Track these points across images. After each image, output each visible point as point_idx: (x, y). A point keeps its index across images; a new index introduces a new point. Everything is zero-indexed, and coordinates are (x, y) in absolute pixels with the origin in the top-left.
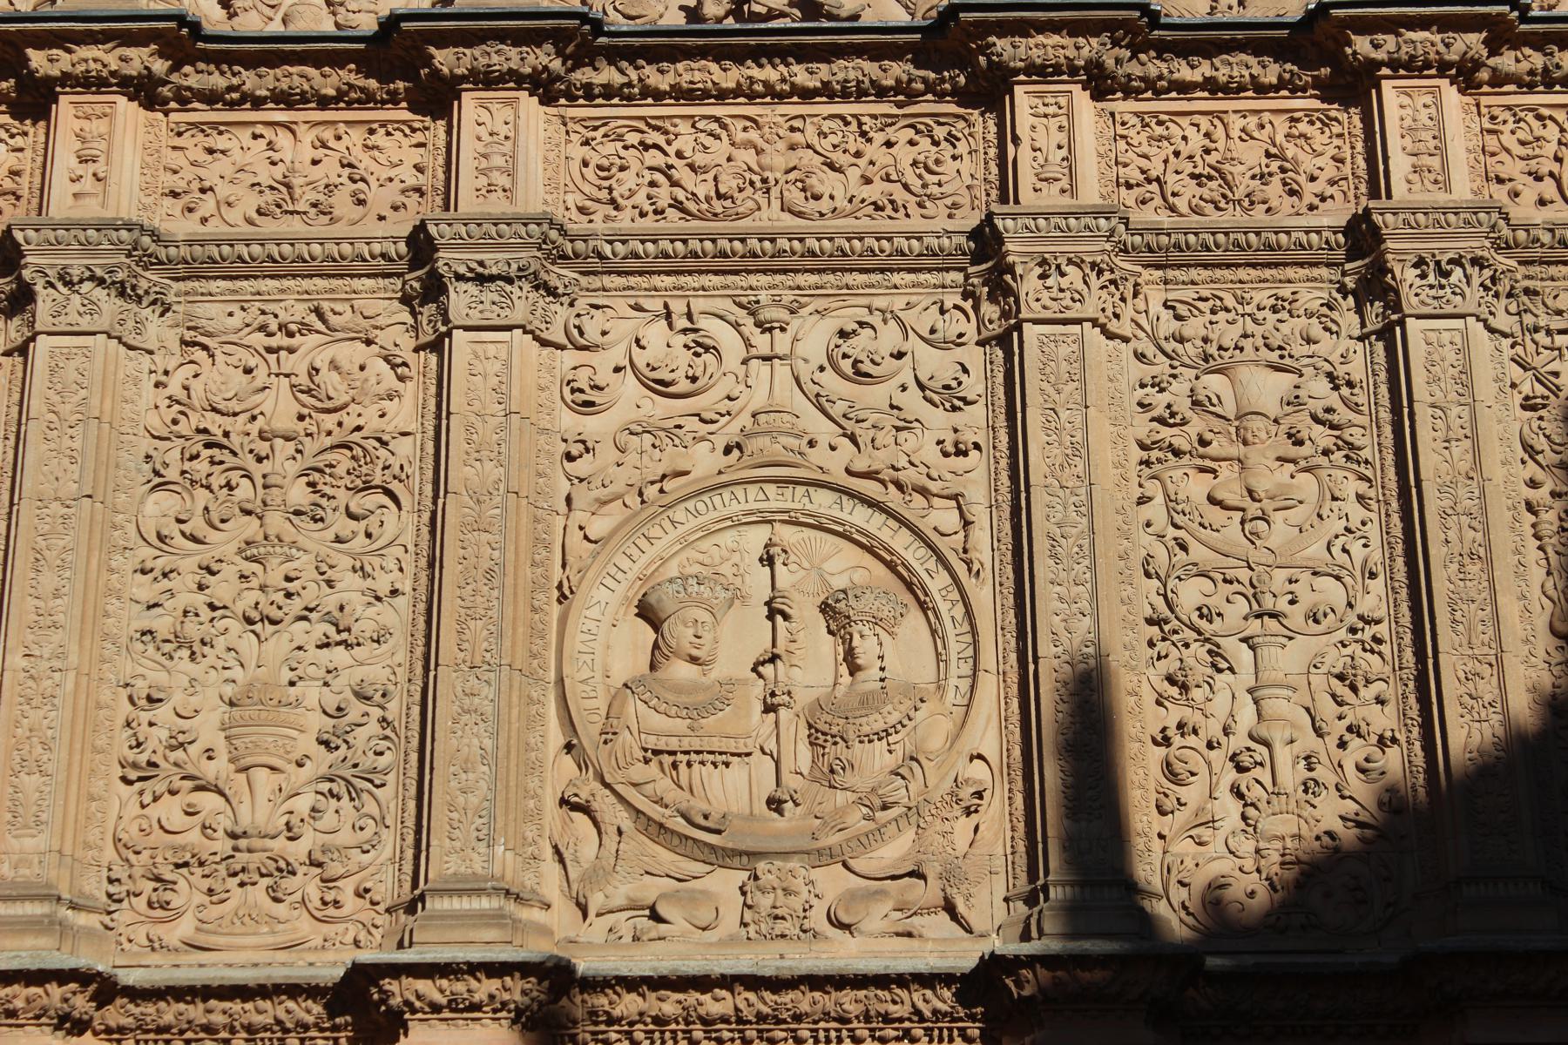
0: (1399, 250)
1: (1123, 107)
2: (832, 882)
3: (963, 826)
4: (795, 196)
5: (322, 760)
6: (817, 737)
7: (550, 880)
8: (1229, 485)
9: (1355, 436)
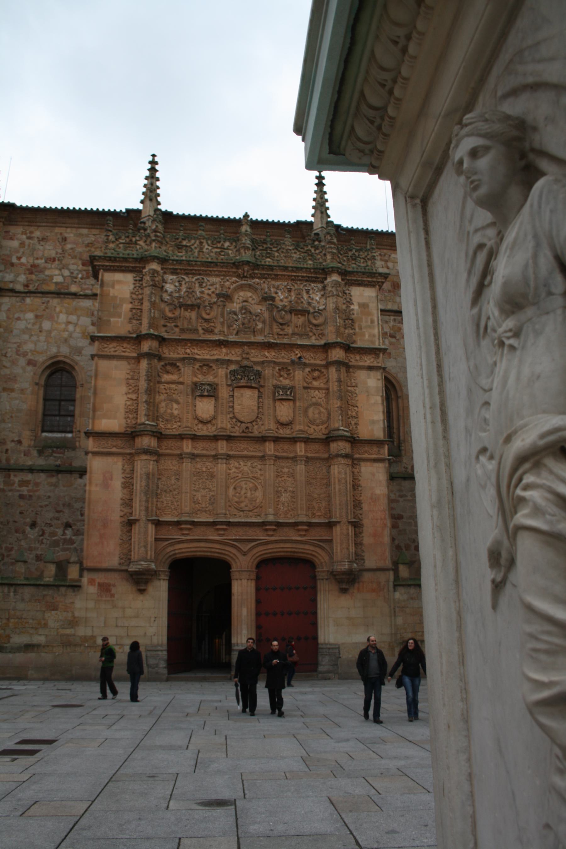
2: (251, 513)
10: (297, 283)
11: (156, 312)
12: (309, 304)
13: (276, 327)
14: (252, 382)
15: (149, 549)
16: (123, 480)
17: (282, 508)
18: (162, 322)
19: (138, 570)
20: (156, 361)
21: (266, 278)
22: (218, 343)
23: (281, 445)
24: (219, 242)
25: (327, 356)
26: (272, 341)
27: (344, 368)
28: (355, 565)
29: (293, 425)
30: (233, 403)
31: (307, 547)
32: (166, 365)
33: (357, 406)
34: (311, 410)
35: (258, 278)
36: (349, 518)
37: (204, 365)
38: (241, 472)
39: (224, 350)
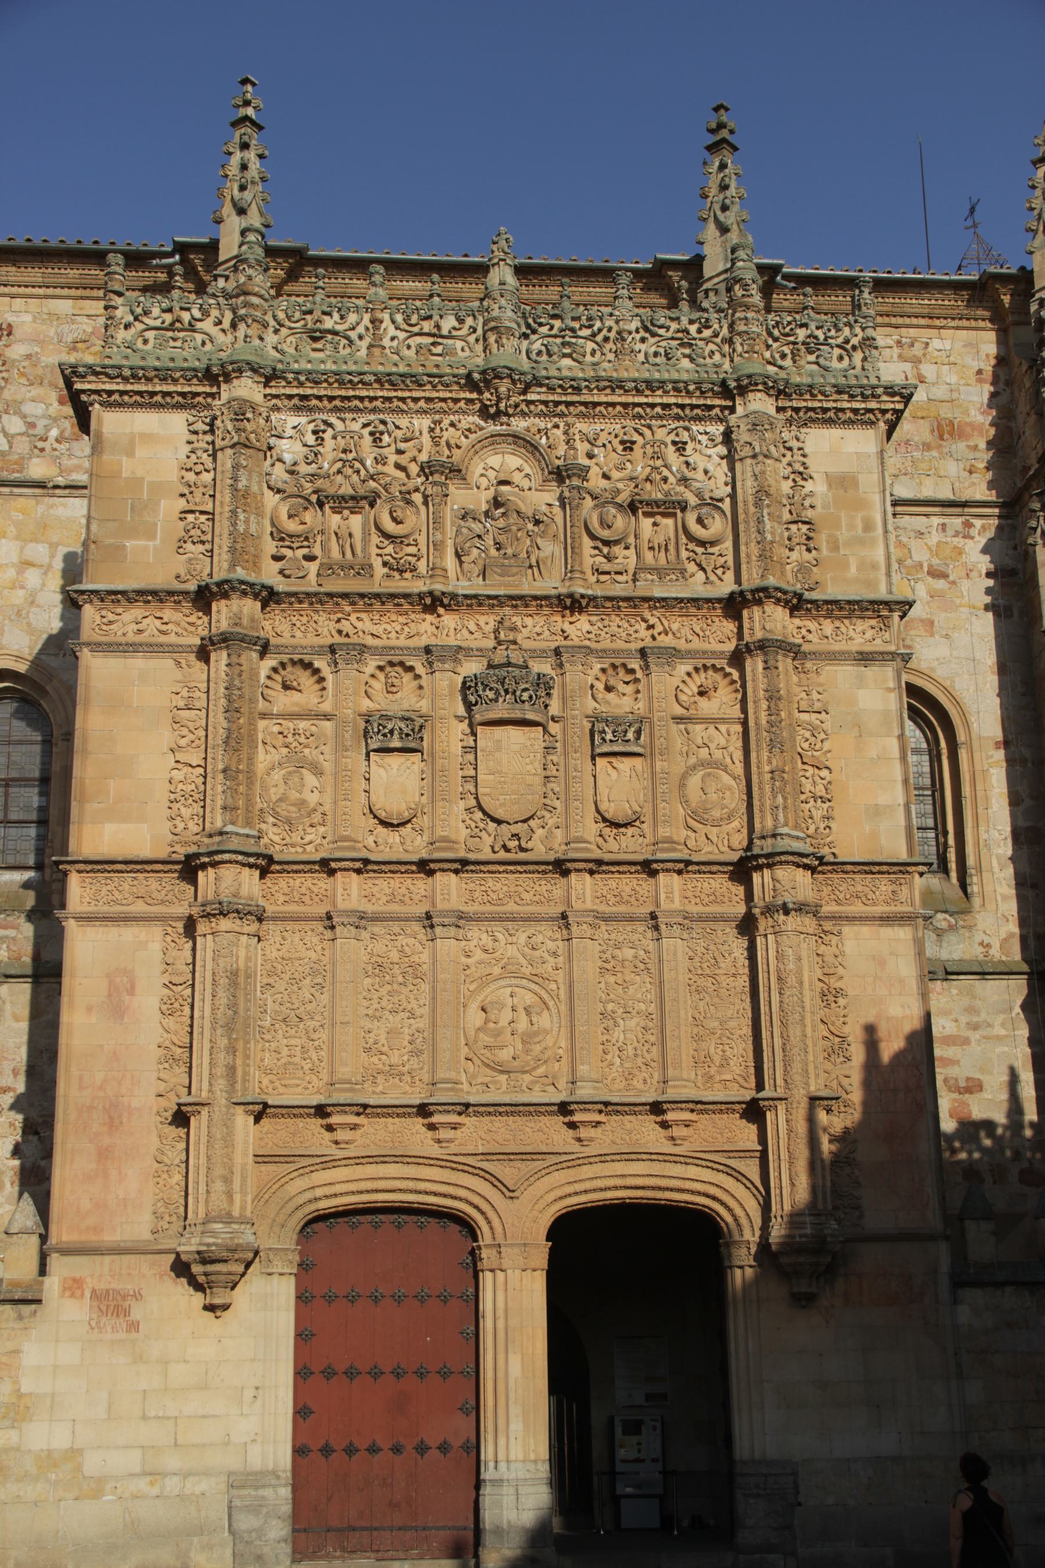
0: (661, 919)
1: (596, 876)
2: (527, 1078)
3: (557, 1064)
4: (517, 899)
5: (410, 1047)
6: (523, 1042)
7: (464, 1079)
8: (619, 978)
9: (649, 966)
10: (649, 427)
11: (252, 518)
12: (684, 481)
13: (597, 552)
14: (527, 705)
15: (236, 1186)
16: (166, 991)
18: (270, 547)
19: (204, 1248)
20: (255, 655)
21: (561, 415)
22: (428, 601)
23: (613, 884)
24: (430, 317)
25: (740, 628)
26: (582, 591)
27: (789, 661)
28: (834, 1225)
29: (644, 826)
30: (476, 769)
31: (692, 1171)
32: (283, 665)
33: (827, 768)
34: (695, 781)
35: (540, 415)
36: (812, 1088)
37: (391, 664)
39: (449, 620)
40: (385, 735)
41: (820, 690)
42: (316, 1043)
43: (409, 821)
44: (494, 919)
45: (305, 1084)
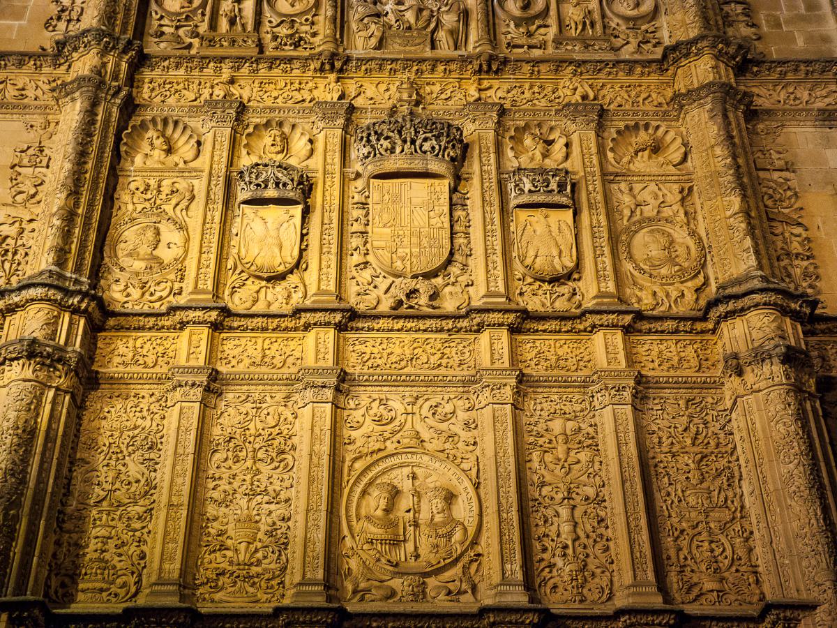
2: (432, 582)
17: (560, 562)
33: (799, 224)
38: (393, 433)
40: (258, 185)
41: (781, 150)
42: (138, 534)
43: (282, 277)
44: (384, 382)
45: (114, 589)
